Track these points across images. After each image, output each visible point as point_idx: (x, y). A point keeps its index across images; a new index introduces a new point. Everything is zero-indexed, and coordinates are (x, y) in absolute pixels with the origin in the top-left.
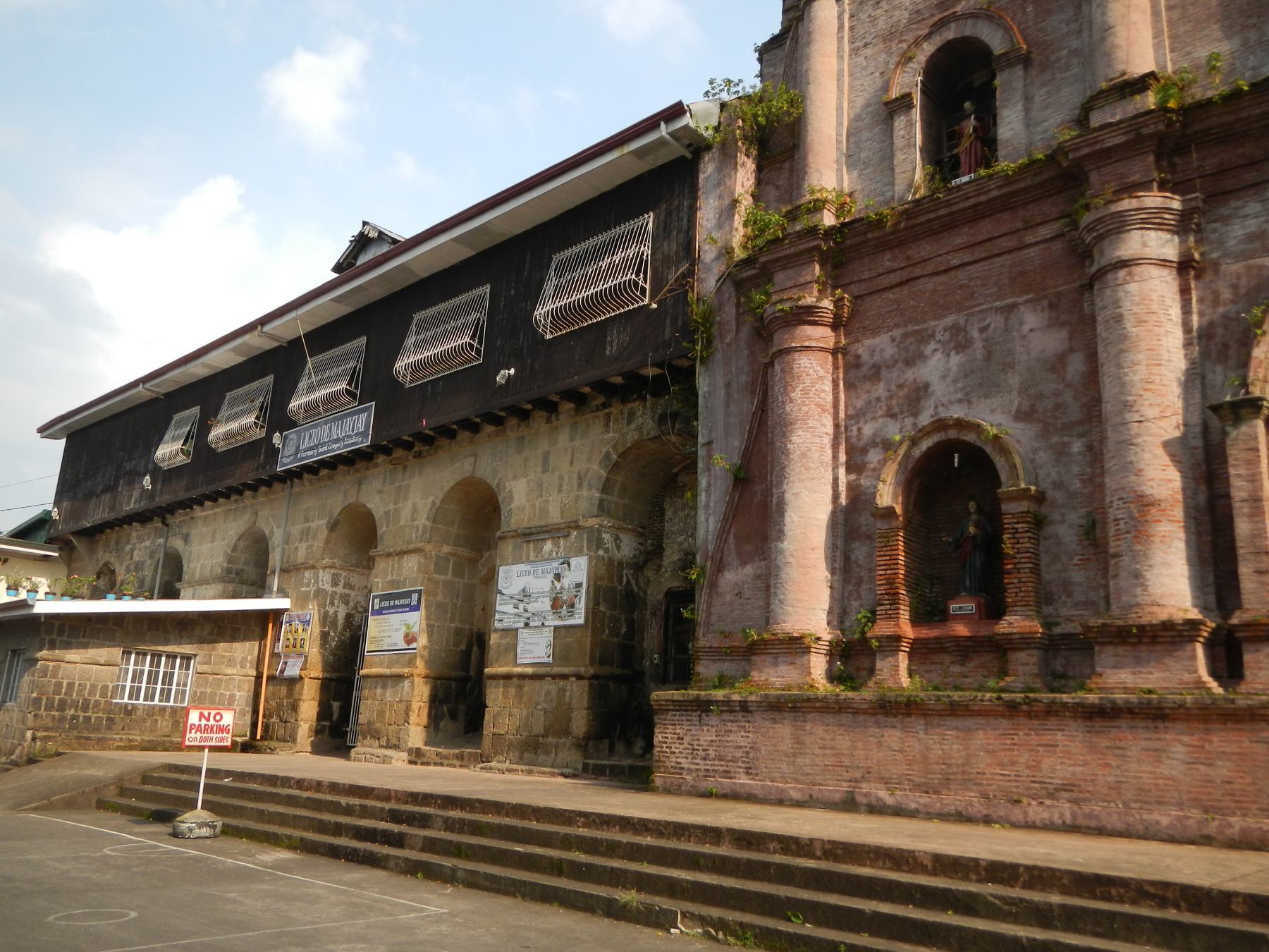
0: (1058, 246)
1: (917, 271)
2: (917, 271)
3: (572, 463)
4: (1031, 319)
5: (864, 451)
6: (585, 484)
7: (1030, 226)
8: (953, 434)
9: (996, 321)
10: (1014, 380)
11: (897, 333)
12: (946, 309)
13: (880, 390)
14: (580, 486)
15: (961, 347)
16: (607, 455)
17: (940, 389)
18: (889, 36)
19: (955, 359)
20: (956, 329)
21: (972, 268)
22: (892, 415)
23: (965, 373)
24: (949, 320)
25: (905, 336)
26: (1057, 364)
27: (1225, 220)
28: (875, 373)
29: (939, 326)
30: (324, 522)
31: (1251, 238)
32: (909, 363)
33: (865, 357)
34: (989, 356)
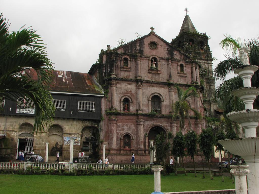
0: (135, 120)
1: (124, 119)
2: (124, 119)
3: (77, 126)
4: (133, 126)
5: (118, 133)
6: (79, 129)
7: (133, 118)
8: (128, 134)
9: (130, 125)
10: (131, 130)
11: (122, 123)
12: (126, 123)
13: (120, 128)
14: (78, 129)
15: (127, 126)
16: (83, 126)
17: (125, 129)
18: (120, 93)
19: (127, 127)
20: (127, 124)
21: (128, 120)
22: (121, 130)
23: (128, 128)
24: (127, 124)
25: (122, 124)
26: (134, 130)
27: (146, 122)
28: (120, 127)
29: (126, 124)
30: (18, 124)
31: (147, 124)
32: (123, 126)
33: (119, 125)
34: (130, 127)
